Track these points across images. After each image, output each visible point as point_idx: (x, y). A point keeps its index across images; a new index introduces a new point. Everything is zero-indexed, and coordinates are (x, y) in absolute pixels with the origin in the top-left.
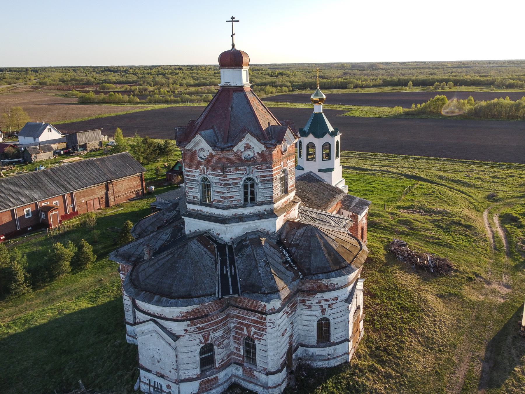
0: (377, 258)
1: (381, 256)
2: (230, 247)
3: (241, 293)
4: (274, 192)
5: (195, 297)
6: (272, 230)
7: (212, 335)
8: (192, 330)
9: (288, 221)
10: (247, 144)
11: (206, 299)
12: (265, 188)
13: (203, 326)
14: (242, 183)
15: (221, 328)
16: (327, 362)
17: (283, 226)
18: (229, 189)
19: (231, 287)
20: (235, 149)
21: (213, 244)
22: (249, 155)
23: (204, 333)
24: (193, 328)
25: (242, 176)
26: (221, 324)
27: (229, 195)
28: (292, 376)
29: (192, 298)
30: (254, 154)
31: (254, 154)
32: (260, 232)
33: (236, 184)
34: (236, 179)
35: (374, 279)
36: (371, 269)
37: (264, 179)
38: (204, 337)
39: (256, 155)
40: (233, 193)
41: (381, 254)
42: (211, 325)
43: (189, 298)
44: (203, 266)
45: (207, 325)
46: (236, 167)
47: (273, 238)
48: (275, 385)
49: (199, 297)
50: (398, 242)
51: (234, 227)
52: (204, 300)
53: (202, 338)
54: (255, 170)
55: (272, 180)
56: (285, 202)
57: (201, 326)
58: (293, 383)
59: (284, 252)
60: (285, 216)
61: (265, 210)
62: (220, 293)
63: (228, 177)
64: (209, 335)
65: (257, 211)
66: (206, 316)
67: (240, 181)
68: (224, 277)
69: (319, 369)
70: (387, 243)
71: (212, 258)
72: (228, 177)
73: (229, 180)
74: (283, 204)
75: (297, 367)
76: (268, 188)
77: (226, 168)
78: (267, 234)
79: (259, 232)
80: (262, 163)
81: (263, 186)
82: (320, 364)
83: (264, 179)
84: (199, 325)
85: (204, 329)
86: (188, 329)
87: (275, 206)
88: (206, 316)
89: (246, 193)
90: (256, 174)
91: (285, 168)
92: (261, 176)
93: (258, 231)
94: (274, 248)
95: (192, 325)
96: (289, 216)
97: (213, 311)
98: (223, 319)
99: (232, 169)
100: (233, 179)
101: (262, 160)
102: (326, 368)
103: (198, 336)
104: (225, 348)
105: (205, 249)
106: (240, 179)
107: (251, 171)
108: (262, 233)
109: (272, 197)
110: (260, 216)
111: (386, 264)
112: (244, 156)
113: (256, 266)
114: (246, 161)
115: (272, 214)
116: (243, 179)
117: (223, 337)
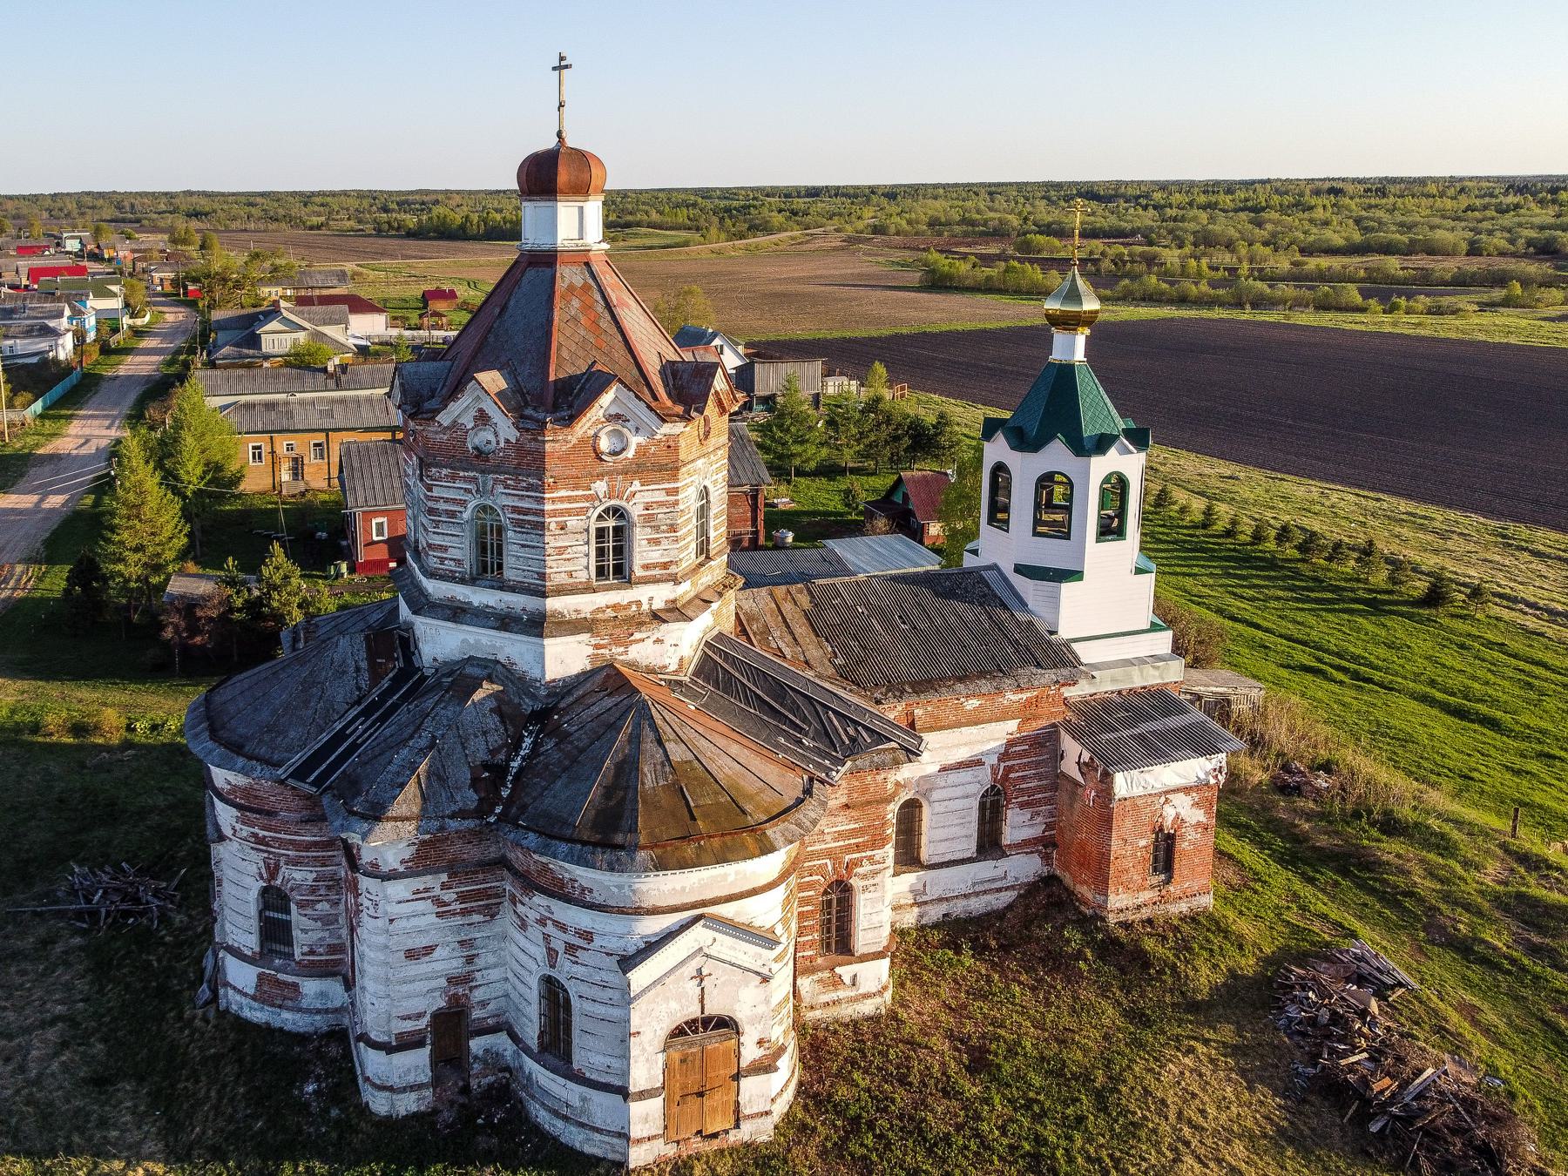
0: (1174, 967)
1: (1205, 970)
2: (424, 678)
3: (325, 790)
4: (549, 563)
5: (244, 756)
6: (535, 673)
7: (285, 871)
8: (244, 834)
9: (612, 666)
10: (481, 411)
11: (259, 768)
12: (523, 546)
13: (265, 837)
14: (466, 515)
15: (307, 865)
16: (560, 1124)
17: (584, 677)
18: (437, 524)
19: (324, 766)
20: (444, 418)
21: (397, 659)
22: (489, 442)
23: (266, 855)
24: (245, 831)
25: (467, 497)
26: (309, 854)
27: (437, 540)
28: (462, 1100)
29: (238, 754)
30: (498, 443)
31: (498, 443)
32: (503, 666)
33: (452, 514)
34: (454, 501)
35: (1067, 1021)
36: (1104, 991)
37: (521, 517)
38: (268, 867)
39: (502, 445)
40: (446, 538)
41: (1215, 966)
42: (283, 844)
43: (233, 751)
44: (321, 698)
45: (274, 839)
46: (452, 468)
47: (534, 697)
48: (378, 1082)
49: (250, 758)
50: (1361, 959)
51: (442, 632)
52: (253, 769)
53: (262, 864)
54: (500, 489)
55: (542, 526)
56: (615, 607)
57: (262, 833)
58: (447, 1115)
59: (528, 741)
60: (597, 647)
61: (524, 609)
62: (291, 770)
63: (436, 493)
64: (277, 867)
65: (503, 606)
66: (270, 814)
67: (462, 509)
68: (340, 737)
69: (537, 1130)
70: (1313, 944)
71: (359, 689)
72: (436, 493)
73: (437, 499)
74: (599, 610)
75: (490, 1086)
76: (533, 547)
77: (430, 465)
78: (520, 678)
79: (499, 667)
80: (516, 472)
81: (520, 539)
82: (543, 1117)
83: (521, 517)
84: (256, 830)
85: (267, 845)
86: (238, 826)
87: (553, 604)
88: (270, 814)
89: (483, 548)
90: (504, 499)
91: (613, 502)
92: (516, 510)
93: (498, 662)
94: (503, 722)
95: (244, 823)
96: (626, 653)
97: (288, 810)
98: (315, 844)
99: (445, 471)
100: (447, 500)
101: (519, 464)
102: (555, 1139)
103: (254, 856)
104: (319, 924)
105: (364, 665)
106: (463, 503)
107: (490, 487)
108: (508, 670)
109: (542, 576)
110: (505, 622)
111: (1194, 1007)
112: (476, 441)
113: (403, 743)
114: (476, 456)
115: (536, 625)
116: (471, 506)
117: (313, 890)
